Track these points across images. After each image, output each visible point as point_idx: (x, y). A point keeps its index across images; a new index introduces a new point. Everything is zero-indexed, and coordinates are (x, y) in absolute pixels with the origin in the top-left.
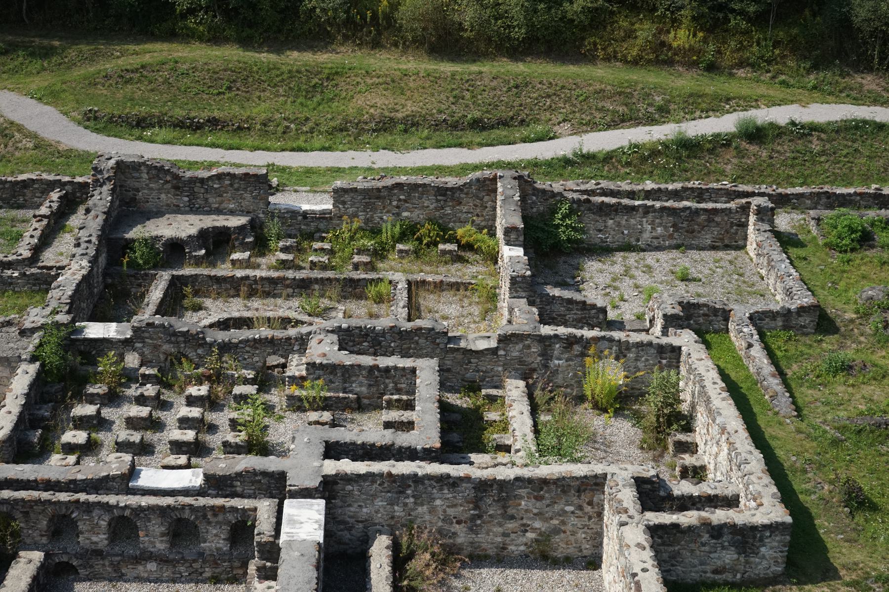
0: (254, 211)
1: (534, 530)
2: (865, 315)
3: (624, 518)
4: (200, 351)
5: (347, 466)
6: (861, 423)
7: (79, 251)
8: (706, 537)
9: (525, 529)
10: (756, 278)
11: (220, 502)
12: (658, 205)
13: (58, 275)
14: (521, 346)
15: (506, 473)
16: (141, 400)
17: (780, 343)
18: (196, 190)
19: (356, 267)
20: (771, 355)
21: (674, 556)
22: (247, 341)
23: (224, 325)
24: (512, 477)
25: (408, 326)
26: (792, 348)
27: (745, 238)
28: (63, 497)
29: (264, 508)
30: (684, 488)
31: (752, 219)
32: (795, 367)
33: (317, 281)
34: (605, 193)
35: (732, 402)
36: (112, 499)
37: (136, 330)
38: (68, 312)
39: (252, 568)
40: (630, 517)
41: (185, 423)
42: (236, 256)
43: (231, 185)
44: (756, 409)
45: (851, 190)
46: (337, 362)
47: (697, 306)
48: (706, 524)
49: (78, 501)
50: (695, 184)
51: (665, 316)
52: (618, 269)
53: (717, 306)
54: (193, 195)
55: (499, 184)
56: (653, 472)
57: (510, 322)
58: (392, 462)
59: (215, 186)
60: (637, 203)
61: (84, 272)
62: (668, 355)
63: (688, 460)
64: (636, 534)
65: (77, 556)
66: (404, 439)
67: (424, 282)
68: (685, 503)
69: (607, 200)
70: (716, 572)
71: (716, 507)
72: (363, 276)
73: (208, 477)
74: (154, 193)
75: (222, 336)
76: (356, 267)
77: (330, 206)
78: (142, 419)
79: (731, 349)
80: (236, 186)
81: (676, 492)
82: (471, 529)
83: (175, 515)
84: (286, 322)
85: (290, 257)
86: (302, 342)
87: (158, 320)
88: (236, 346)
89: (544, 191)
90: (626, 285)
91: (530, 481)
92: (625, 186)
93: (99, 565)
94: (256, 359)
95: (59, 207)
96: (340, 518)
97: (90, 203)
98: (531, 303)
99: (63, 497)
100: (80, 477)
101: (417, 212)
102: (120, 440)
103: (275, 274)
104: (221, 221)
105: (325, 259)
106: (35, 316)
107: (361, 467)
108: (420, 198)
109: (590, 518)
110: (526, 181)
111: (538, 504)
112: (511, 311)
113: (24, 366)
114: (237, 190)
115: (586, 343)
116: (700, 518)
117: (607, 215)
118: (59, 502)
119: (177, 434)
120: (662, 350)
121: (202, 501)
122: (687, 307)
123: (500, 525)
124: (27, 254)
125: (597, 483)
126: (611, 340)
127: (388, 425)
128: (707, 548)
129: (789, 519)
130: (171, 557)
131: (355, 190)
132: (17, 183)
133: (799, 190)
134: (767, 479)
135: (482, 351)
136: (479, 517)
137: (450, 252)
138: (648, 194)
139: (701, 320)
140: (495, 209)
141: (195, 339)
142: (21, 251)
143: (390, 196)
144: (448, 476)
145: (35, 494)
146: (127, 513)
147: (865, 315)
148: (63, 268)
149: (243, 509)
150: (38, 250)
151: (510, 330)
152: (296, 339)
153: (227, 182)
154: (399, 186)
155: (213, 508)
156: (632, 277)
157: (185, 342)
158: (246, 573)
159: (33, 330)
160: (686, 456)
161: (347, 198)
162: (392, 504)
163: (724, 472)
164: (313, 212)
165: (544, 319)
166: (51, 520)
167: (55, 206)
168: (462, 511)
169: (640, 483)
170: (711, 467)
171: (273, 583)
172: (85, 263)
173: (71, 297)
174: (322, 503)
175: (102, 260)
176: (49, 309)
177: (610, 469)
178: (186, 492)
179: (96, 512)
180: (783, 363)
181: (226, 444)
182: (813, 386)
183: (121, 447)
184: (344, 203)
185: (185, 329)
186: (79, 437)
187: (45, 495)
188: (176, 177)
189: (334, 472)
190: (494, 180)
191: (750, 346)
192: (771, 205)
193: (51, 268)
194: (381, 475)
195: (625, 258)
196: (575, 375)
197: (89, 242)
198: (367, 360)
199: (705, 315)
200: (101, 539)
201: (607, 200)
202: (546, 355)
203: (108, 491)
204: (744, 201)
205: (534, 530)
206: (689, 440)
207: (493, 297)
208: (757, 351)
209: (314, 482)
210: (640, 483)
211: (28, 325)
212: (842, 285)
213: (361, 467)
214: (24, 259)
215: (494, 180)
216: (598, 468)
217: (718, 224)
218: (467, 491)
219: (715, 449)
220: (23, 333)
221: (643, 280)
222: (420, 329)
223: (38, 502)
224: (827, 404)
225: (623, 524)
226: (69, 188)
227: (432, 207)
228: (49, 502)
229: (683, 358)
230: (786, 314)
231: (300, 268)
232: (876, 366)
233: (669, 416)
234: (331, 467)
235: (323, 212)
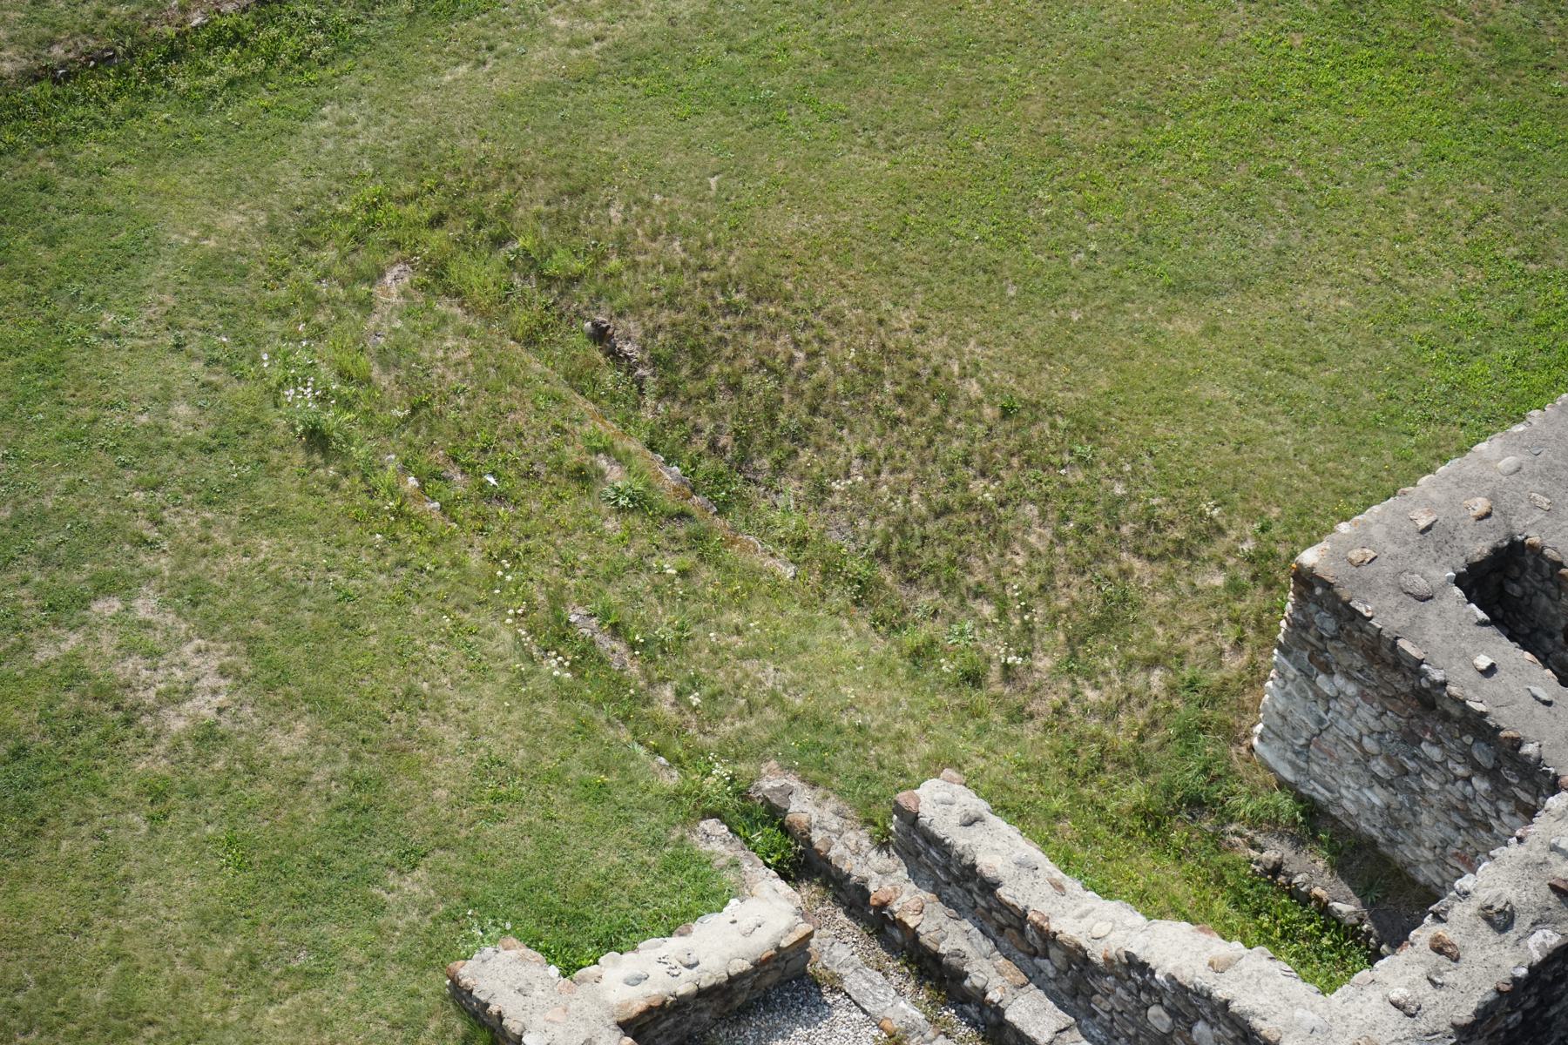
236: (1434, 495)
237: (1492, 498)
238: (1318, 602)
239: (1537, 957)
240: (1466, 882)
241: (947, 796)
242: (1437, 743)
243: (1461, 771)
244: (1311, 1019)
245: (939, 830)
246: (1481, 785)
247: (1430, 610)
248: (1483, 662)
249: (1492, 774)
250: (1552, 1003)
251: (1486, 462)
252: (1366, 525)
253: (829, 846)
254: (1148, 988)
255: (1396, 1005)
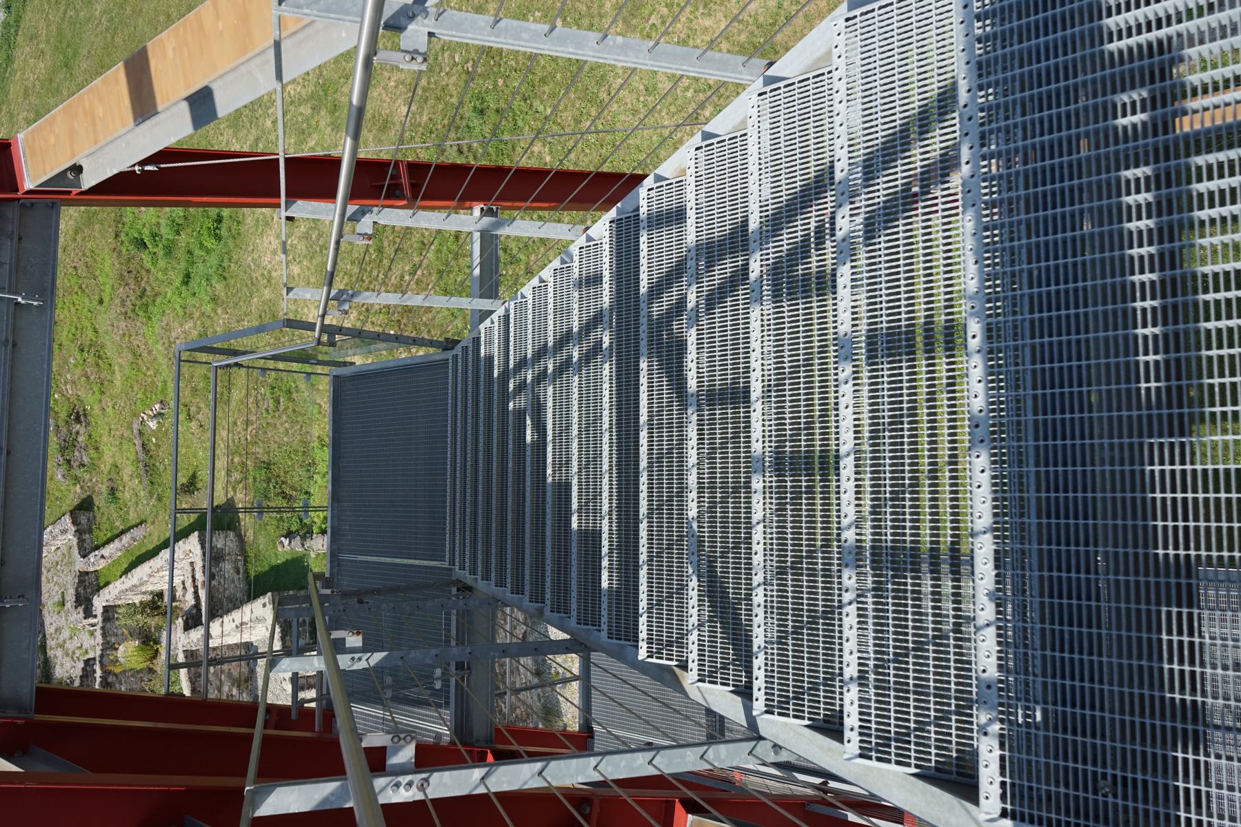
1: (230, 690)
2: (77, 479)
6: (146, 482)
10: (59, 552)
17: (101, 534)
20: (109, 541)
21: (230, 600)
26: (103, 527)
32: (117, 524)
44: (144, 550)
52: (59, 653)
70: (238, 573)
79: (108, 568)
90: (70, 646)
129: (196, 533)
147: (77, 479)
156: (64, 642)
169: (187, 628)
177: (181, 649)
180: (116, 532)
182: (127, 513)
191: (103, 557)
195: (51, 649)
196: (132, 676)
205: (230, 690)
208: (106, 551)
210: (187, 628)
212: (57, 494)
221: (66, 634)
224: (137, 504)
230: (79, 533)
232: (109, 473)
233: (152, 609)
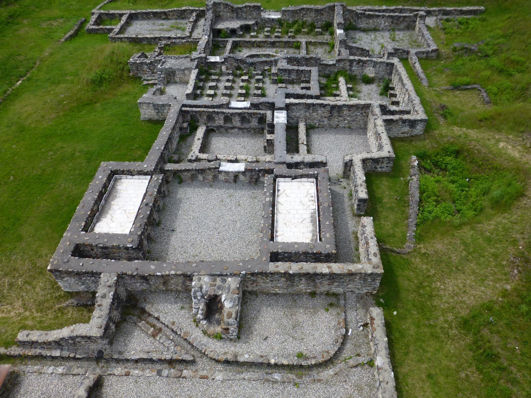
0: (257, 18)
1: (347, 120)
3: (376, 117)
4: (245, 65)
5: (292, 101)
7: (205, 33)
8: (401, 123)
9: (345, 120)
11: (255, 111)
12: (387, 14)
13: (199, 42)
14: (343, 63)
15: (339, 103)
16: (228, 81)
18: (239, 11)
19: (289, 37)
22: (259, 62)
23: (252, 56)
24: (342, 104)
25: (308, 56)
27: (415, 26)
28: (211, 110)
29: (269, 113)
30: (394, 108)
31: (418, 19)
33: (278, 42)
34: (370, 10)
35: (410, 81)
36: (224, 111)
37: (225, 59)
38: (204, 53)
39: (266, 131)
40: (378, 117)
41: (242, 88)
42: (252, 34)
43: (250, 10)
45: (452, 8)
46: (287, 68)
47: (398, 50)
48: (401, 119)
49: (214, 111)
50: (400, 7)
51: (388, 53)
53: (406, 50)
54: (237, 14)
55: (336, 8)
56: (385, 103)
57: (339, 55)
58: (306, 99)
59: (245, 10)
60: (381, 14)
61: (207, 40)
62: (390, 66)
63: (394, 99)
64: (380, 122)
65: (216, 127)
66: (309, 92)
67: (311, 42)
68: (393, 113)
69: (370, 13)
70: (402, 133)
71: (404, 114)
72: (292, 40)
73: (251, 104)
74: (225, 13)
75: (251, 60)
76: (289, 37)
77: (279, 17)
78: (229, 86)
80: (251, 10)
81: (392, 109)
82: (328, 120)
83: (243, 115)
84: (268, 56)
85: (269, 34)
86: (276, 62)
87: (229, 55)
88: (255, 63)
89: (350, 10)
91: (348, 105)
92: (377, 8)
93: (221, 130)
94: (262, 67)
95: (196, 19)
96: (290, 116)
97: (206, 17)
98: (346, 49)
99: (211, 110)
100: (214, 104)
101: (308, 18)
102: (224, 93)
103: (264, 40)
104: (247, 23)
105: (280, 34)
106: (195, 55)
107: (297, 101)
108: (310, 13)
109: (364, 117)
110: (345, 7)
111: (349, 112)
112: (339, 51)
113: (193, 71)
114: (252, 11)
115: (364, 62)
116: (400, 118)
117: (370, 18)
118: (209, 112)
119: (240, 91)
120: (388, 64)
121: (250, 111)
122: (396, 50)
123: (337, 118)
124: (188, 34)
125: (368, 106)
126: (372, 61)
127: (302, 88)
128: (400, 126)
130: (242, 127)
131: (289, 11)
132: (181, 11)
133: (434, 9)
134: (421, 106)
135: (331, 65)
136: (331, 116)
137: (319, 32)
138: (384, 11)
139: (400, 54)
140: (334, 16)
141: (242, 61)
142: (186, 34)
143: (300, 12)
144: (323, 104)
145: (202, 109)
146: (229, 114)
148: (200, 39)
149: (263, 114)
150: (191, 33)
151: (340, 57)
152: (274, 61)
153: (248, 9)
154: (303, 9)
155: (254, 113)
157: (240, 62)
158: (263, 132)
159: (195, 59)
160: (394, 98)
161: (286, 13)
162: (306, 112)
163: (406, 103)
164: (276, 19)
165: (351, 54)
166: (207, 117)
167: (195, 18)
168: (327, 114)
170: (402, 102)
171: (272, 135)
172: (206, 37)
173: (204, 48)
174: (286, 111)
175: (211, 36)
176: (199, 52)
178: (245, 108)
179: (220, 115)
181: (255, 94)
183: (224, 95)
184: (285, 15)
185: (240, 58)
186: (212, 92)
187: (205, 110)
188: (232, 7)
189: (289, 103)
190: (334, 6)
192: (425, 14)
193: (196, 39)
194: (303, 103)
197: (207, 30)
198: (296, 68)
199: (401, 53)
200: (221, 122)
201: (370, 13)
202: (351, 66)
203: (223, 108)
204: (416, 13)
205: (347, 120)
206: (395, 93)
207: (333, 47)
209: (283, 106)
211: (193, 58)
213: (297, 101)
214: (188, 36)
215: (334, 6)
216: (368, 102)
217: (406, 21)
218: (328, 108)
219: (403, 96)
220: (192, 60)
222: (312, 57)
223: (203, 111)
225: (375, 119)
226: (198, 12)
227: (313, 16)
228: (207, 112)
229: (394, 67)
231: (272, 38)
234: (288, 101)
235: (278, 18)
236: (61, 246)
237: (70, 241)
238: (55, 272)
239: (112, 297)
240: (97, 295)
241: (22, 335)
242: (83, 277)
243: (89, 278)
244: (88, 329)
245: (25, 340)
246: (93, 278)
247: (70, 263)
248: (81, 264)
249: (93, 276)
250: (120, 298)
251: (66, 237)
252: (54, 257)
253: (10, 353)
254: (66, 340)
255: (98, 318)
